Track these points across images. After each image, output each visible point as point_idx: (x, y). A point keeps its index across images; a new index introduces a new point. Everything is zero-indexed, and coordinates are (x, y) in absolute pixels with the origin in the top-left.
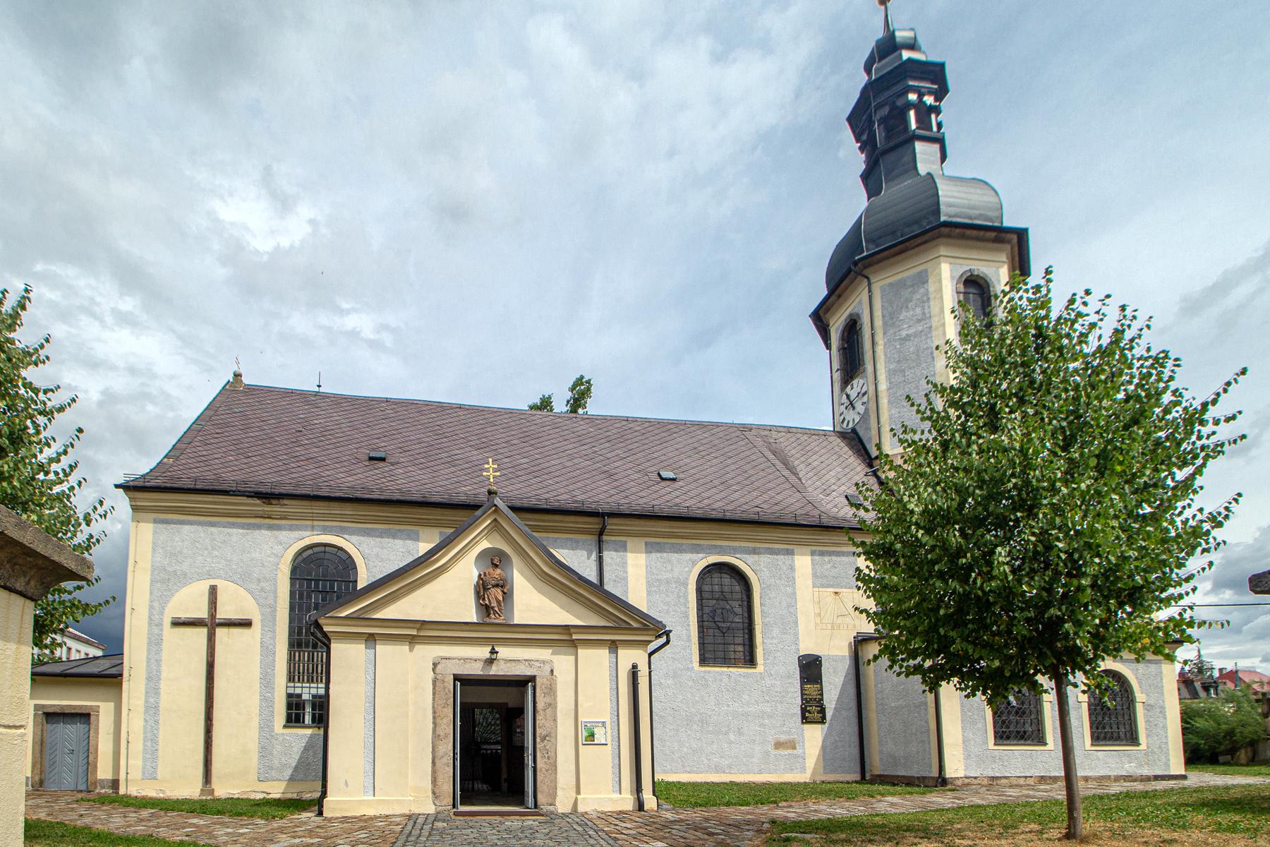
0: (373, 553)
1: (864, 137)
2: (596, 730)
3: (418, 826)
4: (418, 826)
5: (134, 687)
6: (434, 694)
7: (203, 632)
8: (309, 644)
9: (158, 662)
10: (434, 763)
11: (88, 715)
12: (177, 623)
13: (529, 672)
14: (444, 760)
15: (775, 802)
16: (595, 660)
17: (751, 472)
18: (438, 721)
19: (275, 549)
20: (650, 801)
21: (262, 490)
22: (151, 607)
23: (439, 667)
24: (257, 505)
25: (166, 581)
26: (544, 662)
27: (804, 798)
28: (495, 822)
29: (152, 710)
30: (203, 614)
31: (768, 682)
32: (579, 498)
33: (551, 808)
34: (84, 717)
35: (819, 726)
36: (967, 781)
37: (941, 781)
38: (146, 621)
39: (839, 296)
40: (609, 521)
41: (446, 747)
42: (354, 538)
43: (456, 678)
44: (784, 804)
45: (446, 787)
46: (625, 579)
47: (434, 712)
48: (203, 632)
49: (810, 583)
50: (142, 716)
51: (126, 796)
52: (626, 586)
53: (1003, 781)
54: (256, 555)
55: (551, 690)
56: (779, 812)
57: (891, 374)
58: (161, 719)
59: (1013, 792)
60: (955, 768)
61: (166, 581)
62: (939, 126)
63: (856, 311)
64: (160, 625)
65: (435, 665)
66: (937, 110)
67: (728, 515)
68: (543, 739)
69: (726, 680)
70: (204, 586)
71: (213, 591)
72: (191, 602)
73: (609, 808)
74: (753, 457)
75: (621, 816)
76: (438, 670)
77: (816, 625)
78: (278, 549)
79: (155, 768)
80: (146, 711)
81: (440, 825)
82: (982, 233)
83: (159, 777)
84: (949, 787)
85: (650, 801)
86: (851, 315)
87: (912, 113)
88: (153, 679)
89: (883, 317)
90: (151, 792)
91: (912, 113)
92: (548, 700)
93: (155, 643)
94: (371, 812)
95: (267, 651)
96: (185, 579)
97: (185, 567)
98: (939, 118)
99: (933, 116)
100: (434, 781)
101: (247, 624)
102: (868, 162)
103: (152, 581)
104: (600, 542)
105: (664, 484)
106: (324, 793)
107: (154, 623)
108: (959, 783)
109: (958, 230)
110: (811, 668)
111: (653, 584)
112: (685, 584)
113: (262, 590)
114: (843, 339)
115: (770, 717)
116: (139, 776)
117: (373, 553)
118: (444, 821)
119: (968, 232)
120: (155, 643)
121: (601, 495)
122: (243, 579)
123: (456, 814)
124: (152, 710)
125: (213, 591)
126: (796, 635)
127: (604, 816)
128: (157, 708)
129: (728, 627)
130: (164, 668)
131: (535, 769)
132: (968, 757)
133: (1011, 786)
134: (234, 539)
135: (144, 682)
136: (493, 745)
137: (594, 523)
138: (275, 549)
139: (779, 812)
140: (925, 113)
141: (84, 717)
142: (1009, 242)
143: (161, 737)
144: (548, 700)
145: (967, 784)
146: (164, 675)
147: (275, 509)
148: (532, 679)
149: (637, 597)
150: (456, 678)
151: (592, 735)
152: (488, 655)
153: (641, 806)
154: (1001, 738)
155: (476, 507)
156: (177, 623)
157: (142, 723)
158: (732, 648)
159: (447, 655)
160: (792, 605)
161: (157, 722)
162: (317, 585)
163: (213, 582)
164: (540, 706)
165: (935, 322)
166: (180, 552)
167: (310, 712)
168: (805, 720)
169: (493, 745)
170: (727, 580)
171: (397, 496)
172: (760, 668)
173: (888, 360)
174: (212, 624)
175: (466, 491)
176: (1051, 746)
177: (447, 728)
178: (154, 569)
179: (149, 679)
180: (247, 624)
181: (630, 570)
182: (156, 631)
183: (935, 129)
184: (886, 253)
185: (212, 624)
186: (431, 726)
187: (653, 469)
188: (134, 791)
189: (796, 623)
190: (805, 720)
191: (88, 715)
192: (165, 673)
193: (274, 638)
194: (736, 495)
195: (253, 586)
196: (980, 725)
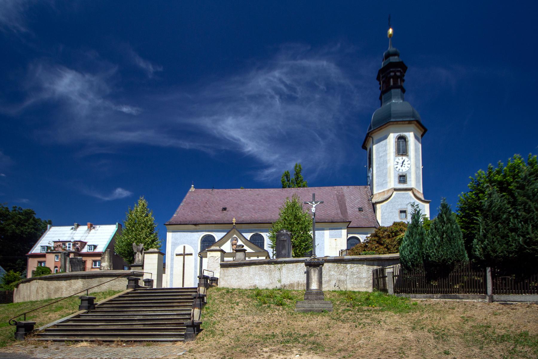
7: (182, 257)
12: (177, 255)
19: (198, 237)
24: (193, 227)
25: (175, 245)
29: (172, 274)
48: (182, 257)
57: (377, 168)
61: (175, 245)
71: (184, 247)
78: (198, 236)
87: (392, 80)
88: (172, 268)
91: (392, 80)
93: (172, 259)
101: (191, 254)
107: (172, 255)
120: (172, 259)
122: (191, 244)
124: (172, 274)
125: (184, 247)
138: (198, 237)
156: (177, 255)
165: (388, 152)
173: (376, 164)
174: (184, 255)
180: (191, 254)
192: (175, 266)
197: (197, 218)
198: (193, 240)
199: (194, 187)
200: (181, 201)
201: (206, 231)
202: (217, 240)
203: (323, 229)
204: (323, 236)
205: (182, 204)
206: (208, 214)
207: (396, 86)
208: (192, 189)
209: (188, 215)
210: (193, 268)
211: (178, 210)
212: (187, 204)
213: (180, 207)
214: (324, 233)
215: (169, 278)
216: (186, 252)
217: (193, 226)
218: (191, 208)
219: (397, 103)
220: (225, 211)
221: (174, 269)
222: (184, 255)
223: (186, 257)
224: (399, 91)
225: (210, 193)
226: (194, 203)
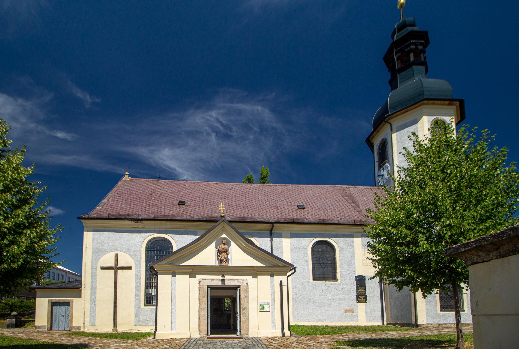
0: (178, 241)
1: (391, 65)
2: (265, 306)
3: (191, 342)
4: (191, 342)
5: (86, 291)
6: (199, 293)
8: (152, 276)
9: (96, 282)
10: (199, 319)
12: (103, 268)
13: (237, 284)
14: (204, 318)
15: (341, 334)
16: (264, 280)
17: (337, 204)
18: (201, 303)
19: (140, 241)
20: (287, 333)
21: (135, 218)
22: (92, 262)
23: (201, 283)
24: (132, 224)
26: (244, 280)
27: (354, 332)
28: (223, 341)
30: (113, 264)
31: (342, 286)
32: (263, 217)
33: (247, 336)
34: (67, 304)
35: (364, 304)
36: (427, 325)
37: (417, 326)
38: (91, 267)
39: (378, 132)
40: (275, 225)
41: (204, 313)
42: (171, 235)
43: (208, 287)
44: (345, 334)
45: (204, 328)
46: (282, 247)
47: (199, 300)
49: (361, 248)
51: (83, 332)
52: (282, 250)
53: (444, 325)
54: (133, 242)
55: (247, 291)
56: (341, 337)
59: (446, 330)
60: (422, 319)
61: (98, 252)
62: (425, 58)
63: (385, 137)
64: (96, 269)
65: (200, 282)
66: (423, 52)
67: (326, 222)
68: (244, 309)
69: (324, 286)
70: (112, 255)
71: (116, 256)
73: (270, 335)
74: (339, 198)
75: (275, 338)
76: (201, 284)
77: (363, 264)
81: (200, 342)
82: (442, 102)
84: (420, 328)
85: (287, 333)
86: (383, 139)
88: (93, 289)
89: (397, 139)
90: (92, 330)
92: (245, 294)
93: (94, 276)
94: (174, 337)
95: (138, 277)
96: (105, 252)
97: (105, 247)
98: (425, 55)
99: (422, 55)
100: (199, 326)
101: (129, 268)
102: (392, 75)
104: (271, 233)
105: (299, 210)
106: (156, 330)
107: (94, 268)
108: (424, 326)
109: (431, 102)
110: (361, 281)
111: (293, 250)
112: (307, 249)
113: (135, 255)
114: (379, 149)
115: (343, 300)
117: (178, 241)
118: (202, 340)
119: (436, 102)
120: (94, 276)
121: (272, 215)
122: (128, 251)
123: (208, 338)
125: (116, 256)
126: (354, 268)
127: (267, 339)
129: (325, 266)
131: (240, 320)
132: (428, 316)
133: (447, 328)
134: (124, 236)
136: (223, 312)
137: (269, 226)
138: (140, 241)
139: (341, 337)
140: (418, 53)
141: (67, 304)
142: (455, 105)
144: (245, 294)
145: (427, 327)
146: (98, 287)
147: (140, 225)
148: (239, 287)
149: (287, 257)
150: (208, 287)
151: (263, 308)
152: (221, 278)
153: (283, 335)
154: (444, 308)
155: (216, 221)
156: (103, 268)
158: (326, 274)
159: (205, 278)
160: (353, 256)
162: (157, 253)
163: (116, 252)
164: (242, 297)
166: (103, 242)
167: (150, 300)
168: (358, 301)
169: (223, 312)
170: (324, 247)
171: (189, 218)
172: (339, 281)
174: (116, 268)
175: (216, 216)
176: (466, 311)
177: (204, 305)
178: (93, 248)
180: (129, 268)
181: (284, 244)
182: (94, 271)
183: (423, 59)
184: (399, 113)
186: (198, 305)
187: (295, 204)
188: (86, 330)
189: (354, 263)
190: (358, 301)
193: (140, 273)
194: (330, 213)
196: (434, 303)
197: (137, 211)
198: (131, 247)
199: (129, 176)
200: (109, 190)
201: (155, 232)
202: (175, 249)
203: (352, 236)
204: (352, 246)
205: (110, 194)
206: (155, 209)
208: (127, 178)
209: (121, 208)
210: (134, 291)
211: (104, 201)
212: (119, 194)
213: (107, 197)
214: (353, 242)
215: (88, 305)
216: (120, 264)
218: (127, 199)
220: (183, 206)
222: (116, 268)
223: (119, 271)
225: (155, 184)
226: (131, 194)
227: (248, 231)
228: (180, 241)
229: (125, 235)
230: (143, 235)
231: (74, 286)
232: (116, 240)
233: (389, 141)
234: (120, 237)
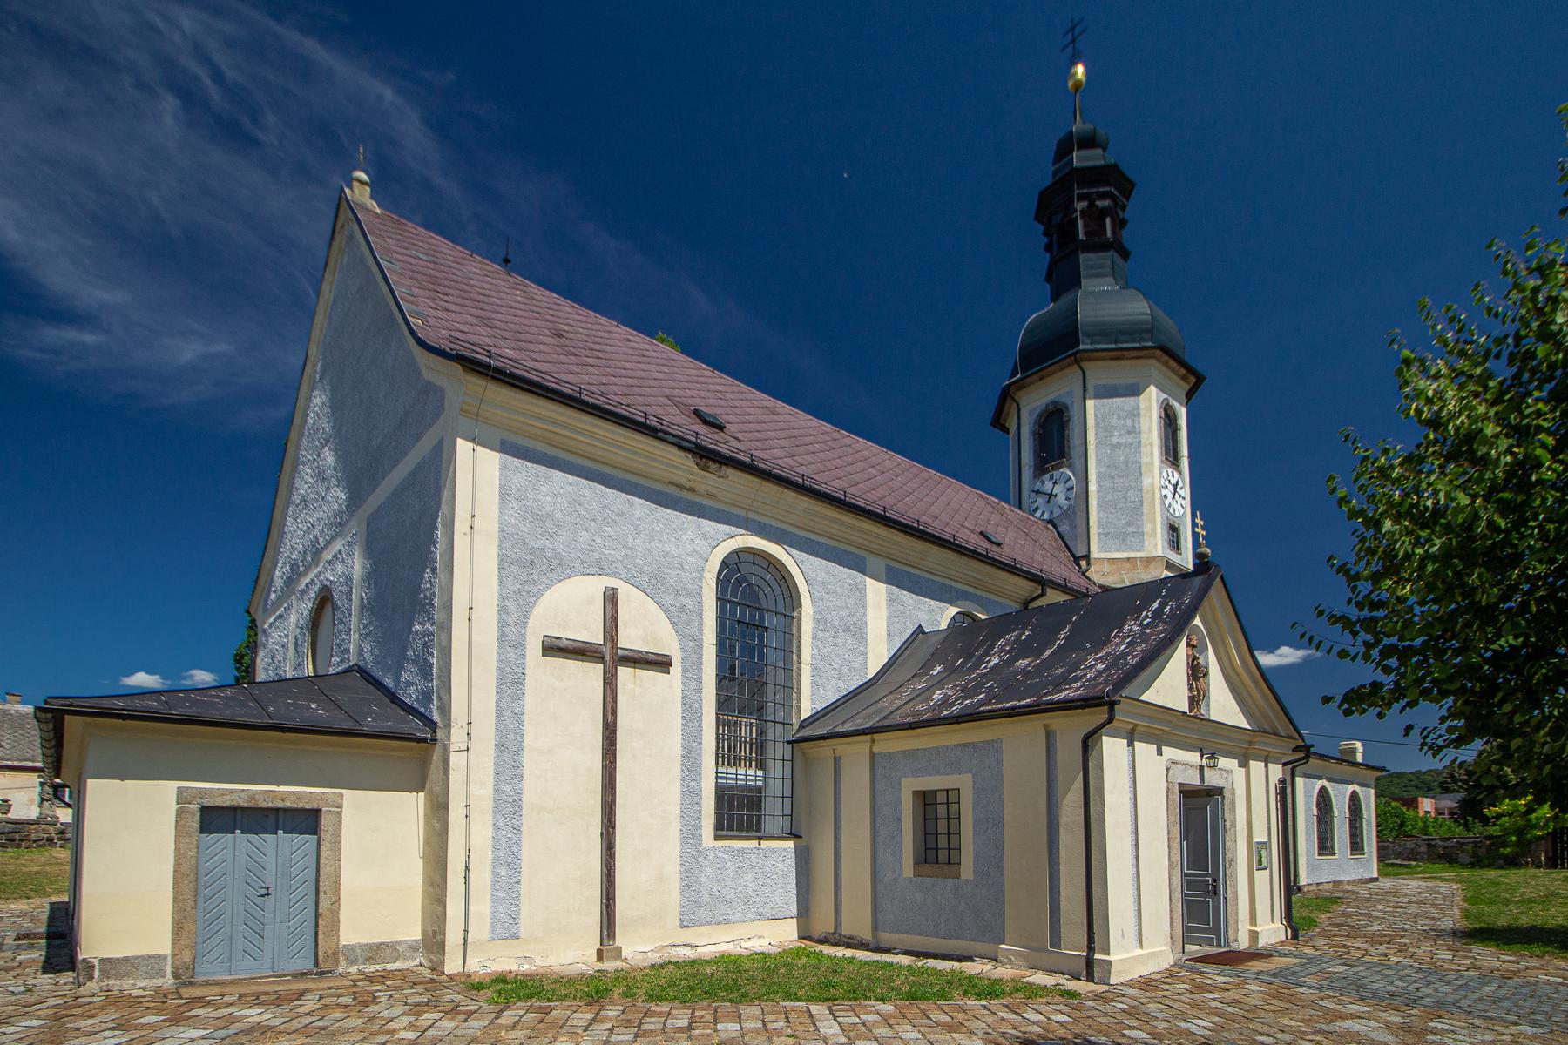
9: (519, 716)
11: (315, 813)
22: (503, 610)
24: (682, 466)
25: (527, 567)
29: (509, 807)
30: (593, 633)
50: (489, 819)
58: (526, 824)
61: (527, 567)
64: (520, 645)
70: (595, 586)
72: (571, 607)
78: (701, 545)
79: (514, 917)
80: (497, 809)
83: (522, 934)
93: (511, 681)
96: (560, 568)
97: (559, 545)
103: (503, 562)
107: (510, 641)
116: (486, 935)
120: (511, 681)
122: (653, 587)
124: (509, 807)
128: (517, 803)
130: (528, 729)
135: (492, 753)
143: (525, 859)
157: (489, 832)
161: (517, 830)
162: (743, 613)
166: (550, 516)
178: (504, 537)
179: (501, 747)
182: (512, 655)
185: (609, 656)
191: (315, 813)
193: (699, 691)
195: (669, 599)
207: (1098, 244)
217: (687, 462)
219: (1104, 299)
221: (530, 763)
224: (1106, 258)
227: (978, 592)
228: (822, 584)
229: (640, 506)
230: (709, 526)
231: (388, 720)
232: (605, 522)
233: (1075, 412)
234: (621, 514)
